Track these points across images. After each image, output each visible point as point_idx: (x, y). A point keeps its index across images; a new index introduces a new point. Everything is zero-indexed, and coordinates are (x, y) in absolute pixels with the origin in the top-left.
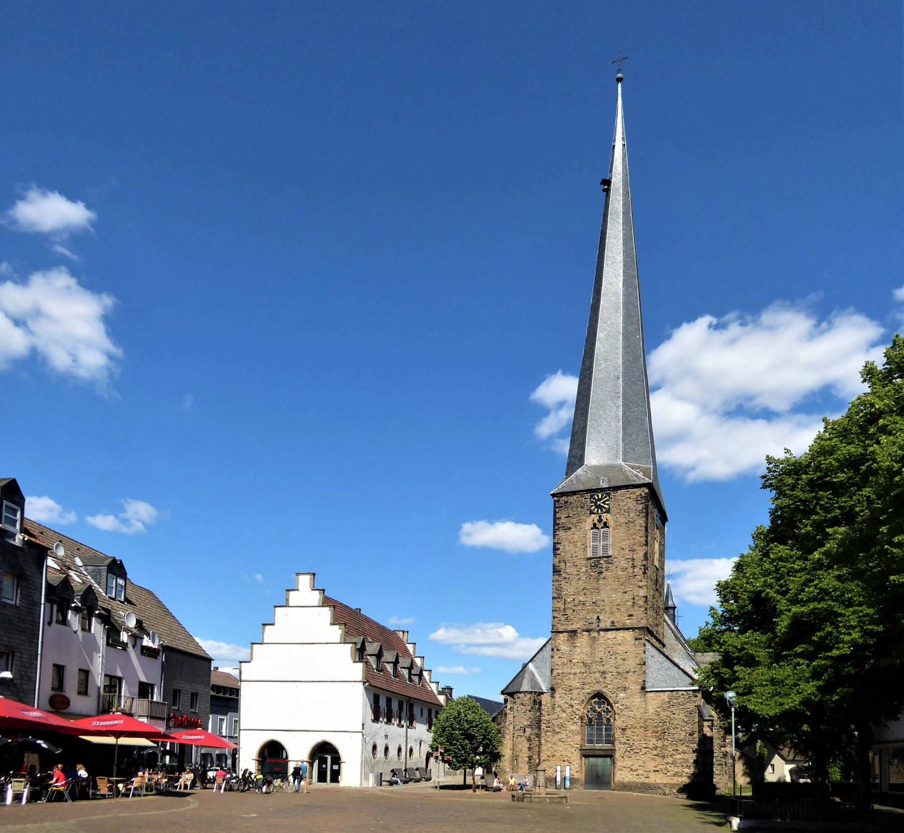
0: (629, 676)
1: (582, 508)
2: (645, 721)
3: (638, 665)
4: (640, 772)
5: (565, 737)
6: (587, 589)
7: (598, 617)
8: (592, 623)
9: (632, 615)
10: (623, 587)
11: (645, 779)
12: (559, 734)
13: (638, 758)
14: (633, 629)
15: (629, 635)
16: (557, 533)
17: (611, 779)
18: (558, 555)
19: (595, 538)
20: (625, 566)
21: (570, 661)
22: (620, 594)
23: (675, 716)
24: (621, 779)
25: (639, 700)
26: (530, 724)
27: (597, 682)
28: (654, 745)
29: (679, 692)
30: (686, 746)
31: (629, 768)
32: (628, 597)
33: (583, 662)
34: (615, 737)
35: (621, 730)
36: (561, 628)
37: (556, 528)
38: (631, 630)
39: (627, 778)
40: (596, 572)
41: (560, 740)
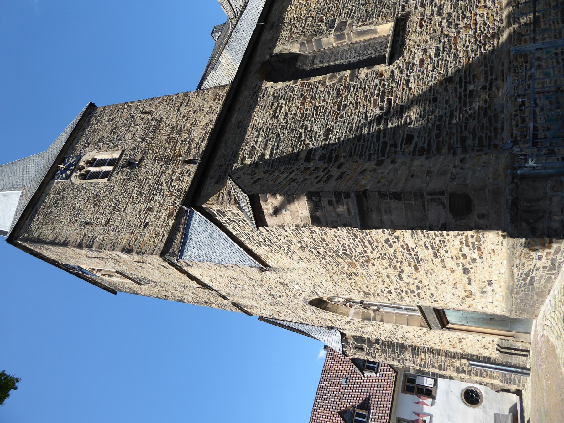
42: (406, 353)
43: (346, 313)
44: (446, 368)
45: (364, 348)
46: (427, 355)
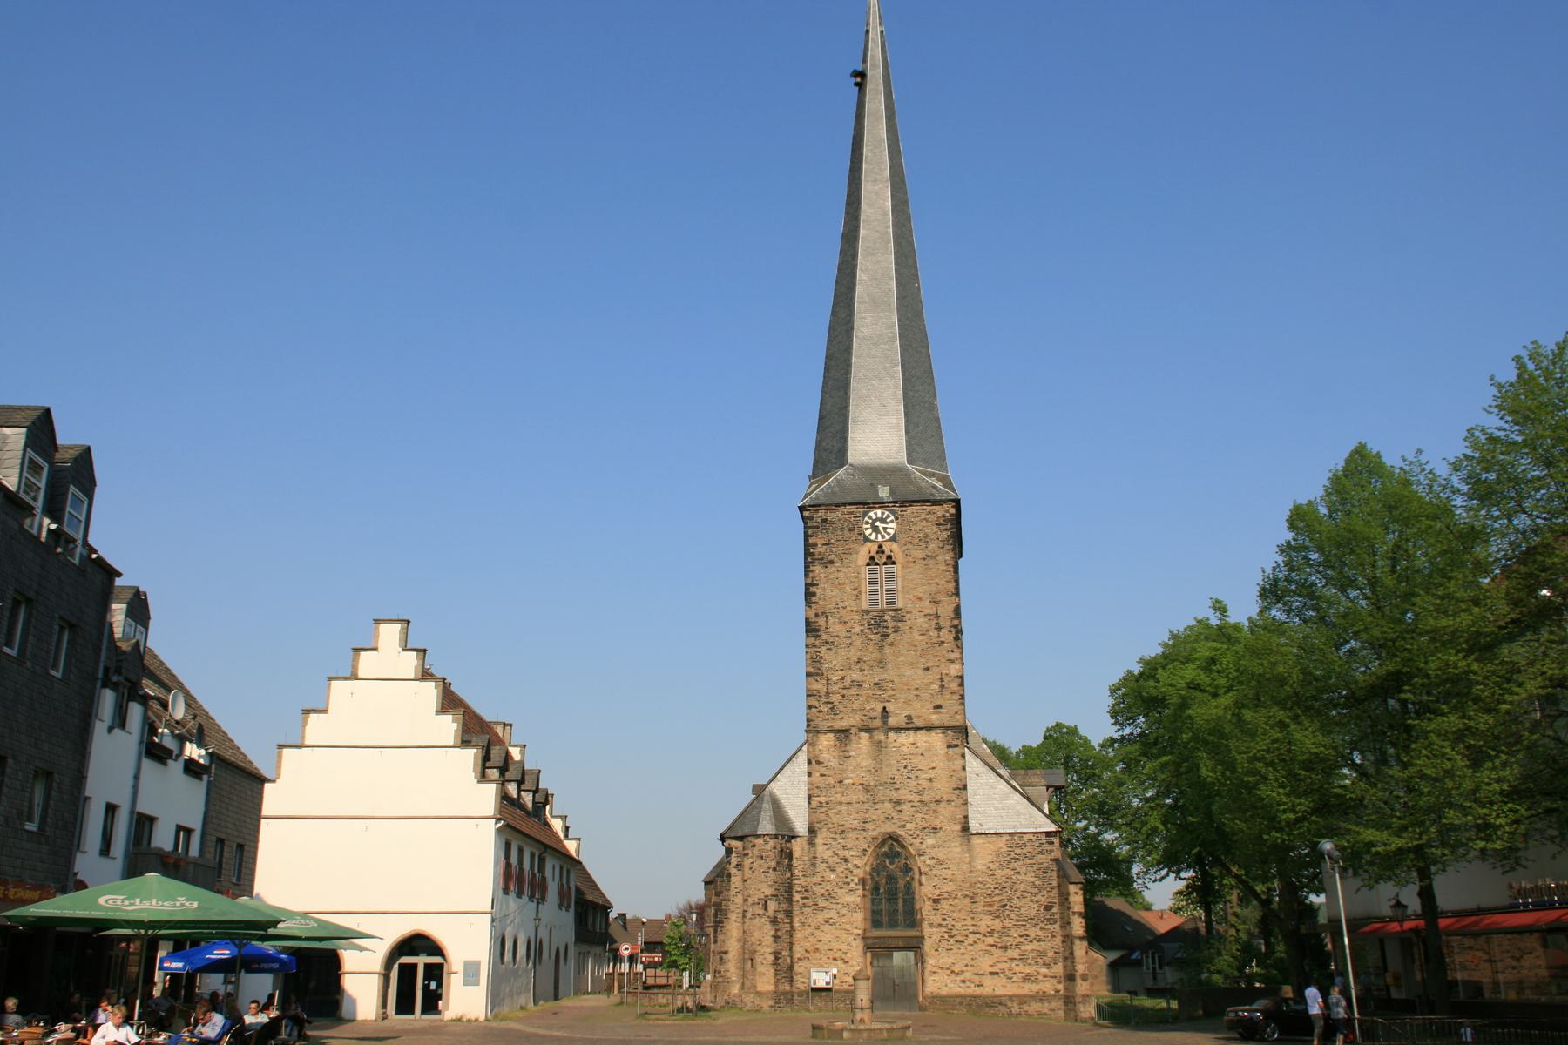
0: (942, 808)
1: (850, 530)
2: (971, 886)
3: (955, 789)
4: (967, 975)
5: (836, 916)
6: (864, 662)
7: (884, 708)
8: (875, 718)
9: (939, 707)
10: (923, 660)
11: (977, 988)
12: (825, 911)
13: (962, 951)
14: (945, 728)
15: (937, 740)
16: (812, 568)
17: (917, 988)
18: (813, 603)
19: (873, 582)
20: (926, 626)
21: (841, 782)
22: (920, 672)
23: (1020, 877)
24: (936, 990)
25: (959, 850)
26: (774, 893)
27: (887, 818)
28: (988, 927)
29: (1024, 835)
30: (1041, 929)
31: (948, 969)
32: (933, 676)
33: (862, 784)
34: (921, 914)
35: (930, 903)
36: (824, 725)
37: (810, 560)
38: (939, 731)
39: (946, 989)
40: (877, 633)
41: (827, 922)
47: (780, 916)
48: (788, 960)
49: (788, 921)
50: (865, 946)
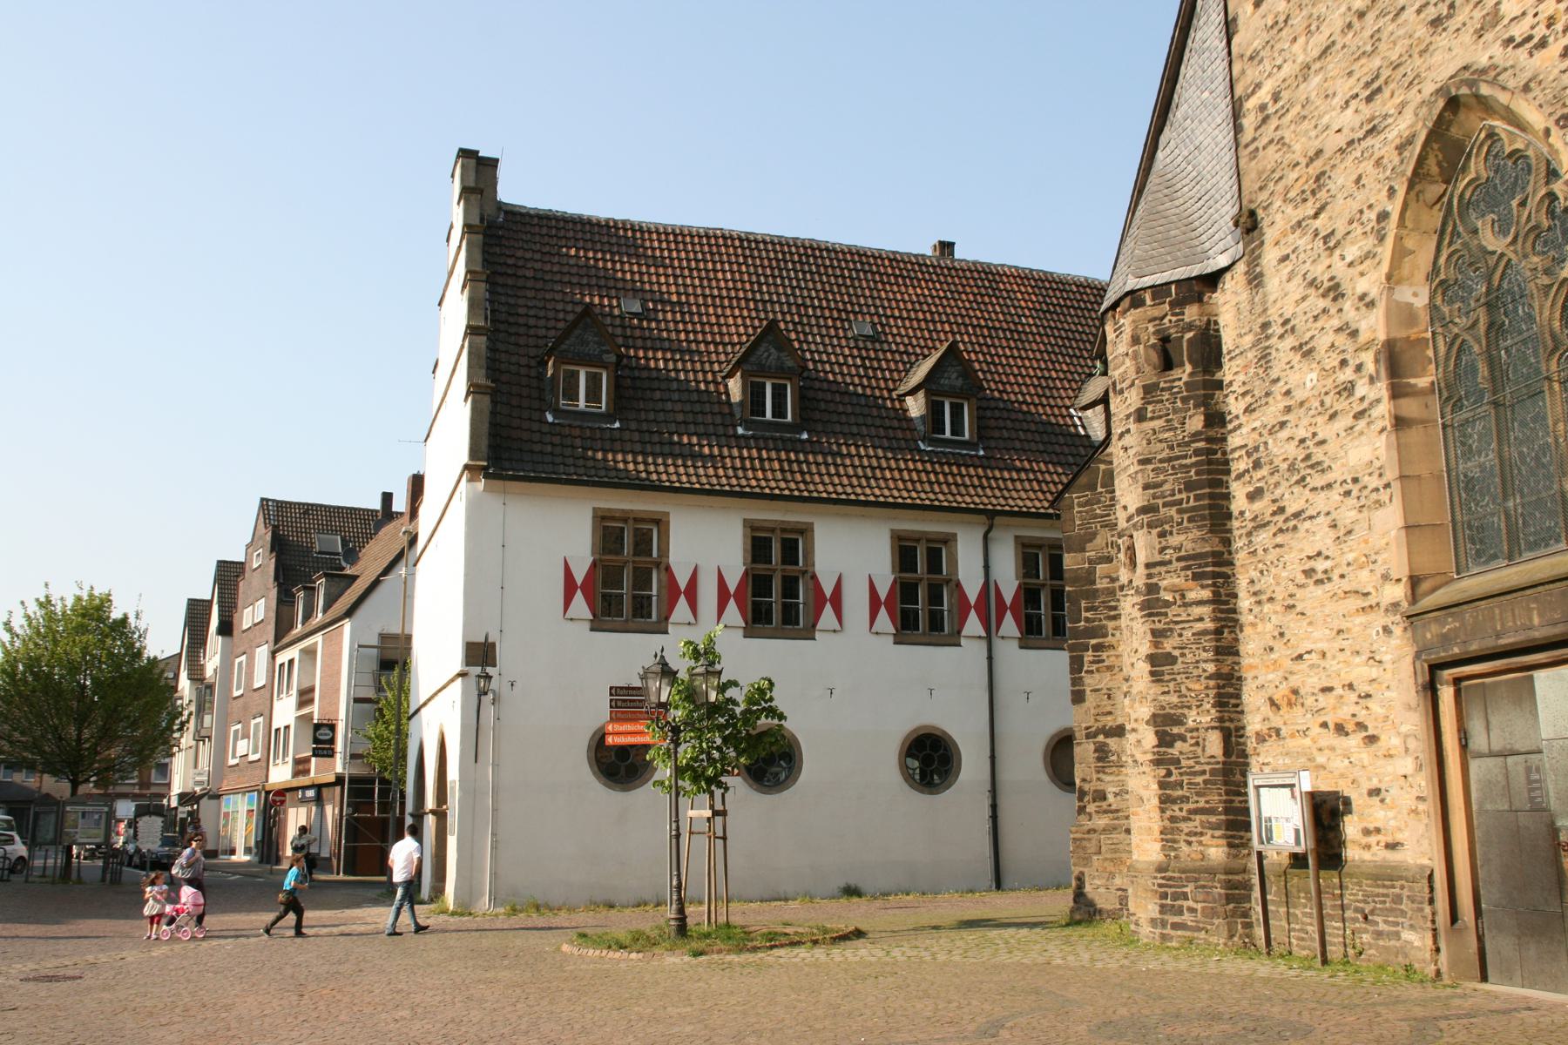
41: (1309, 573)
42: (1196, 534)
43: (1405, 271)
44: (1167, 677)
45: (1176, 373)
46: (1205, 610)
47: (1170, 580)
48: (1214, 744)
49: (1206, 594)
50: (1417, 655)
